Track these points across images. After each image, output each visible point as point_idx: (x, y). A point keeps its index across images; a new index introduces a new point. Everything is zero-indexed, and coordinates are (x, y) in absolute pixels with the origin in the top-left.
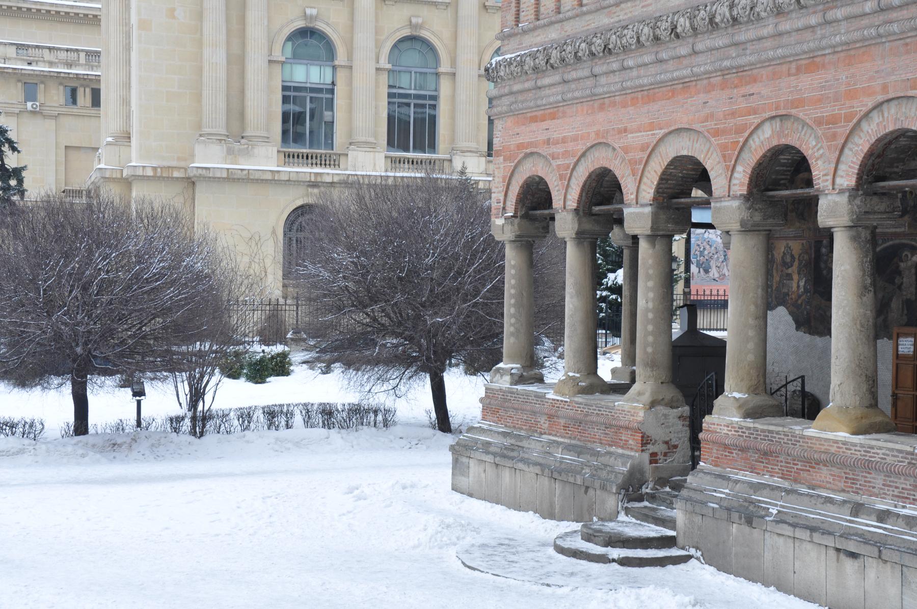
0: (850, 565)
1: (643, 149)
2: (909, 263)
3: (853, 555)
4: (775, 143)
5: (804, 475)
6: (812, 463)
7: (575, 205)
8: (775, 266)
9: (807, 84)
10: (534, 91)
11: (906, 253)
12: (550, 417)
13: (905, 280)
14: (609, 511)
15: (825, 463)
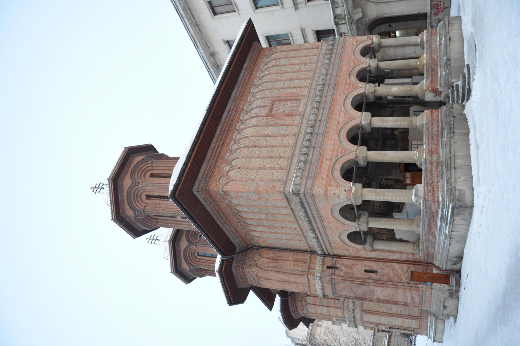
0: (452, 39)
1: (345, 114)
2: (385, 182)
3: (450, 39)
4: (355, 76)
5: (435, 61)
6: (432, 59)
7: (356, 146)
8: (380, 232)
9: (345, 68)
10: (311, 166)
11: (382, 183)
12: (432, 153)
13: (389, 183)
14: (459, 107)
15: (432, 56)
